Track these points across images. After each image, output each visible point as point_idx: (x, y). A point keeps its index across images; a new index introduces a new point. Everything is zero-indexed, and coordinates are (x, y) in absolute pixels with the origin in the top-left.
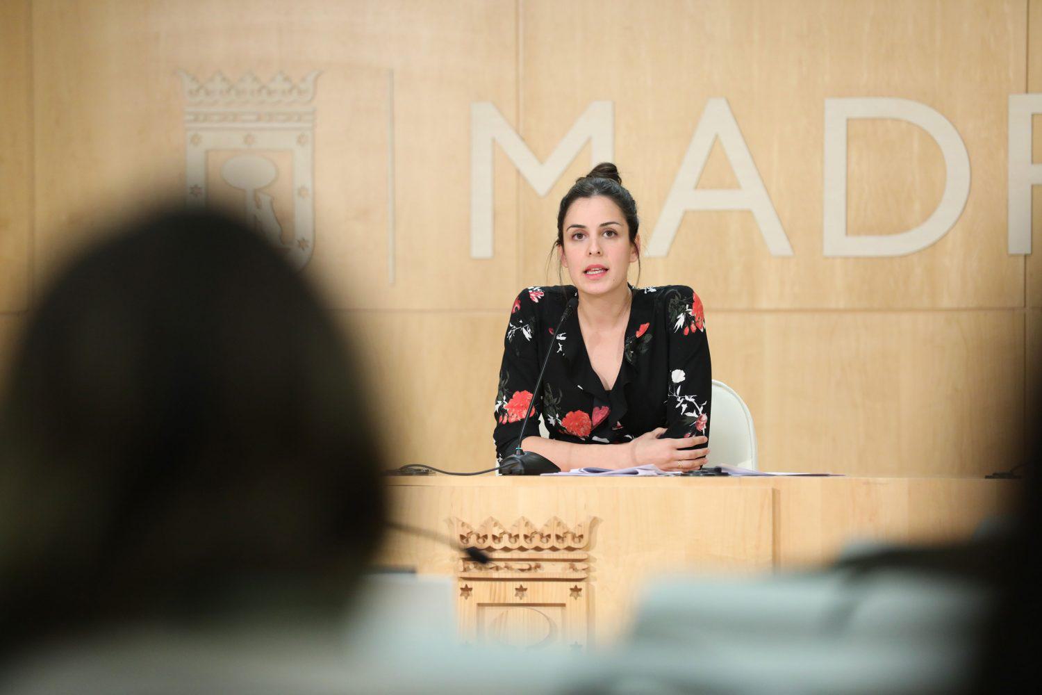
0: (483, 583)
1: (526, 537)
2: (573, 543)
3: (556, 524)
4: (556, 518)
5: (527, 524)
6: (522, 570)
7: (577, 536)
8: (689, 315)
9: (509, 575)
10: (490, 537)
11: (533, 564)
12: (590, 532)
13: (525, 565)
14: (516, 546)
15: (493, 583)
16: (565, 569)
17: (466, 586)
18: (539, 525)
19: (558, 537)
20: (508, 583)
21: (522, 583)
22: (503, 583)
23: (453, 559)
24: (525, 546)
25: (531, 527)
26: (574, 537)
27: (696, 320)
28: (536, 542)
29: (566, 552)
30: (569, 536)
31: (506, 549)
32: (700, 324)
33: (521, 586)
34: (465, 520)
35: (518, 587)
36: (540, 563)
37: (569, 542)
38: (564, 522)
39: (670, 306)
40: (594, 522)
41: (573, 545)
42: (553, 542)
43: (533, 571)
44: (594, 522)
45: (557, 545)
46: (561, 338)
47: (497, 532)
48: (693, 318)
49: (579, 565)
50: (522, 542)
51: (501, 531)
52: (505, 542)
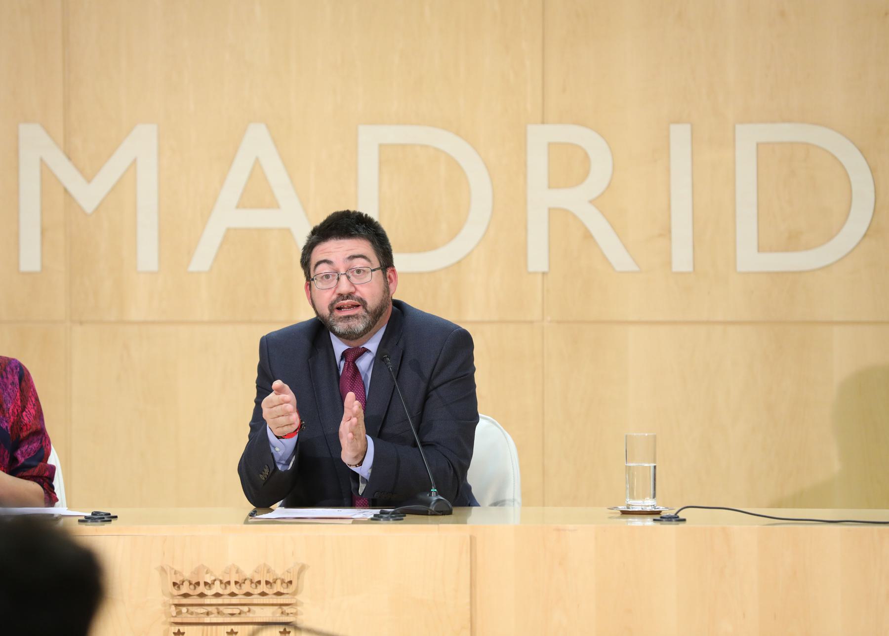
0: (195, 627)
1: (236, 583)
3: (265, 572)
4: (265, 565)
5: (237, 572)
6: (232, 615)
7: (286, 581)
9: (220, 620)
10: (202, 584)
11: (245, 609)
12: (298, 578)
13: (236, 611)
14: (228, 591)
15: (205, 627)
16: (273, 613)
17: (179, 630)
18: (248, 572)
19: (267, 583)
20: (219, 627)
21: (233, 627)
22: (214, 627)
23: (164, 604)
24: (236, 591)
26: (283, 582)
28: (247, 588)
29: (274, 596)
30: (279, 582)
31: (217, 595)
33: (232, 630)
34: (177, 567)
35: (229, 631)
36: (250, 607)
37: (278, 587)
38: (273, 568)
41: (282, 591)
42: (263, 588)
43: (242, 615)
44: (302, 569)
45: (266, 590)
49: (287, 609)
50: (233, 588)
51: (213, 578)
52: (217, 588)
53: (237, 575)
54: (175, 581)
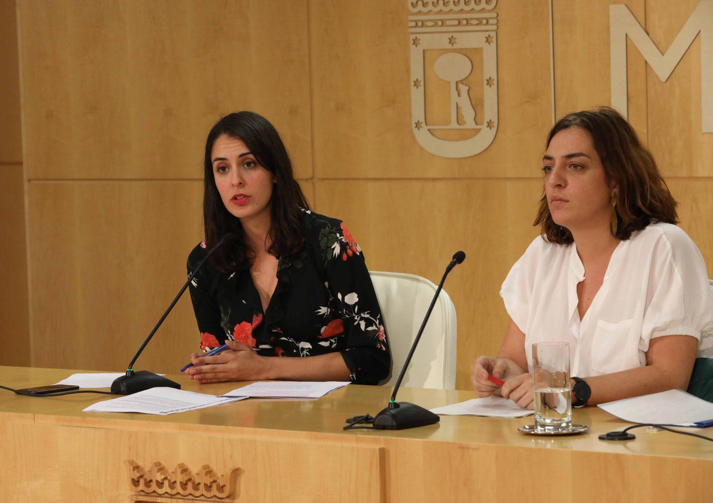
2: (217, 492)
3: (204, 473)
8: (343, 242)
25: (190, 473)
27: (350, 245)
32: (354, 248)
34: (140, 463)
39: (320, 235)
40: (236, 472)
44: (236, 472)
46: (234, 264)
47: (159, 477)
48: (347, 244)
51: (163, 477)
53: (182, 475)
54: (133, 478)
